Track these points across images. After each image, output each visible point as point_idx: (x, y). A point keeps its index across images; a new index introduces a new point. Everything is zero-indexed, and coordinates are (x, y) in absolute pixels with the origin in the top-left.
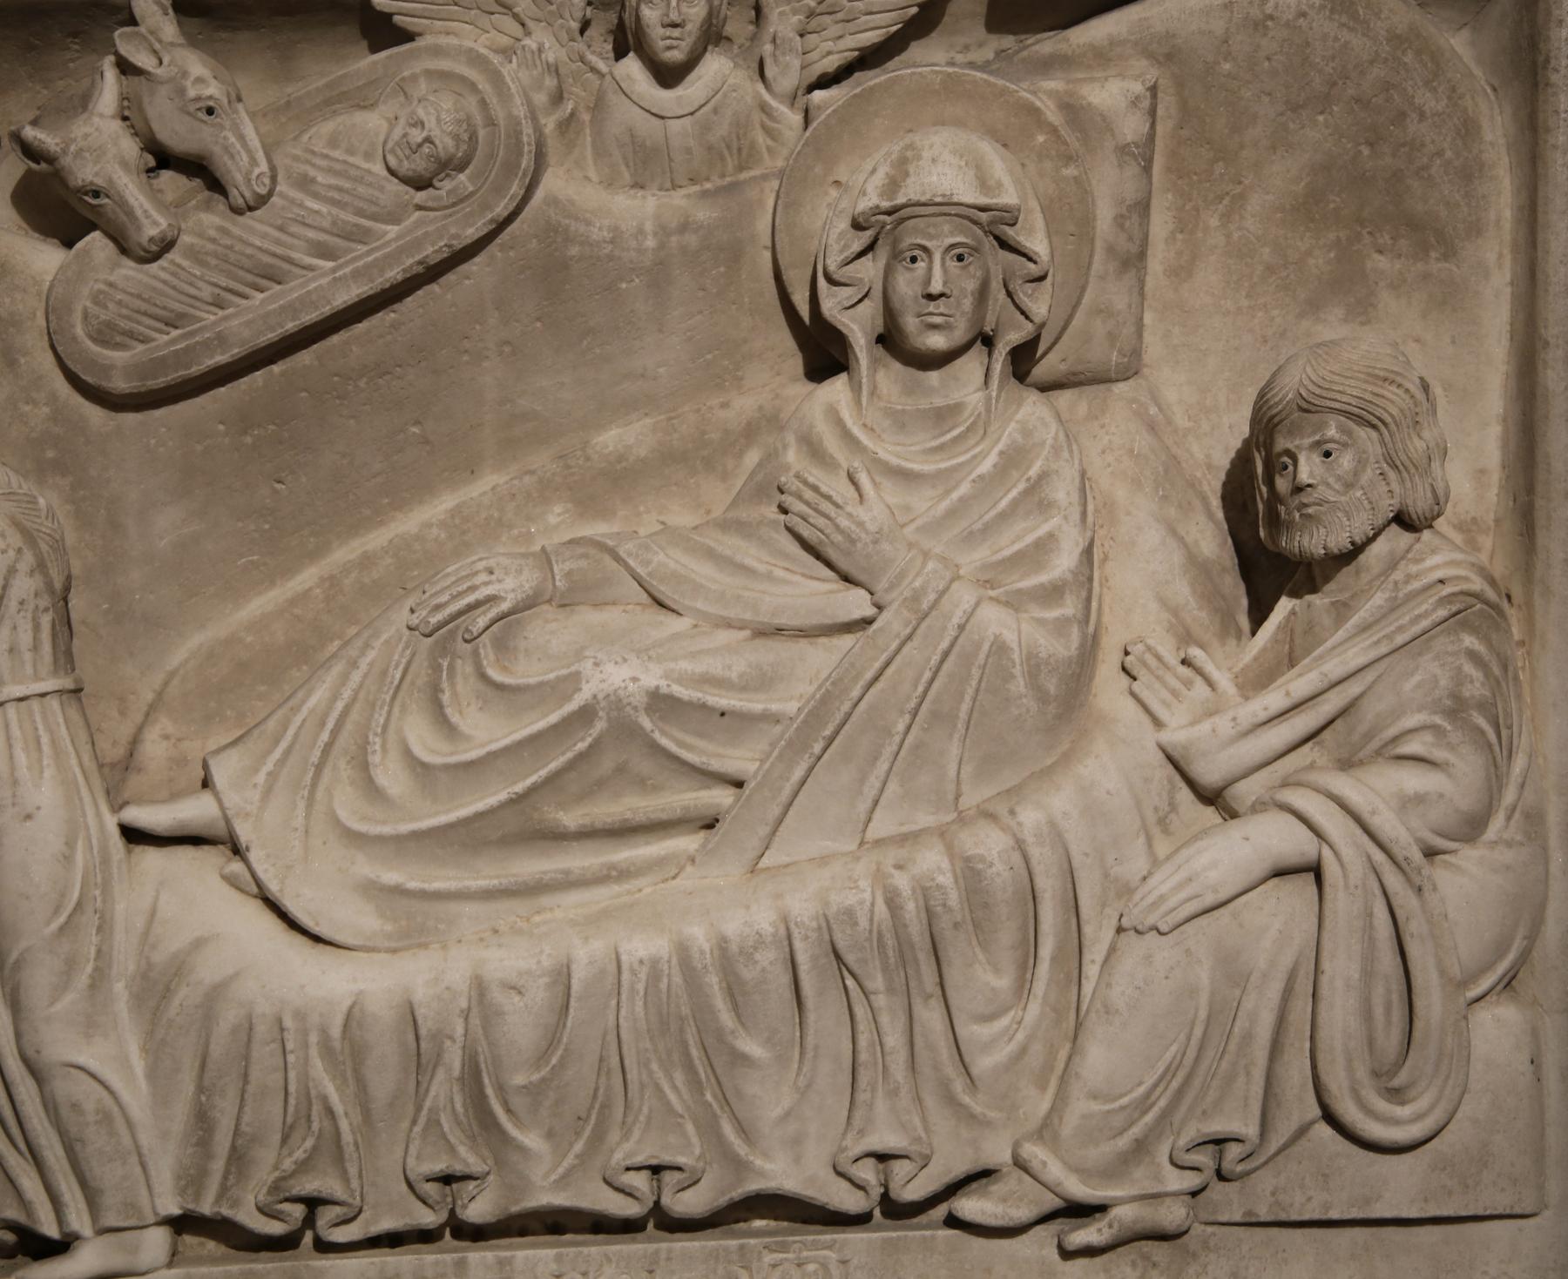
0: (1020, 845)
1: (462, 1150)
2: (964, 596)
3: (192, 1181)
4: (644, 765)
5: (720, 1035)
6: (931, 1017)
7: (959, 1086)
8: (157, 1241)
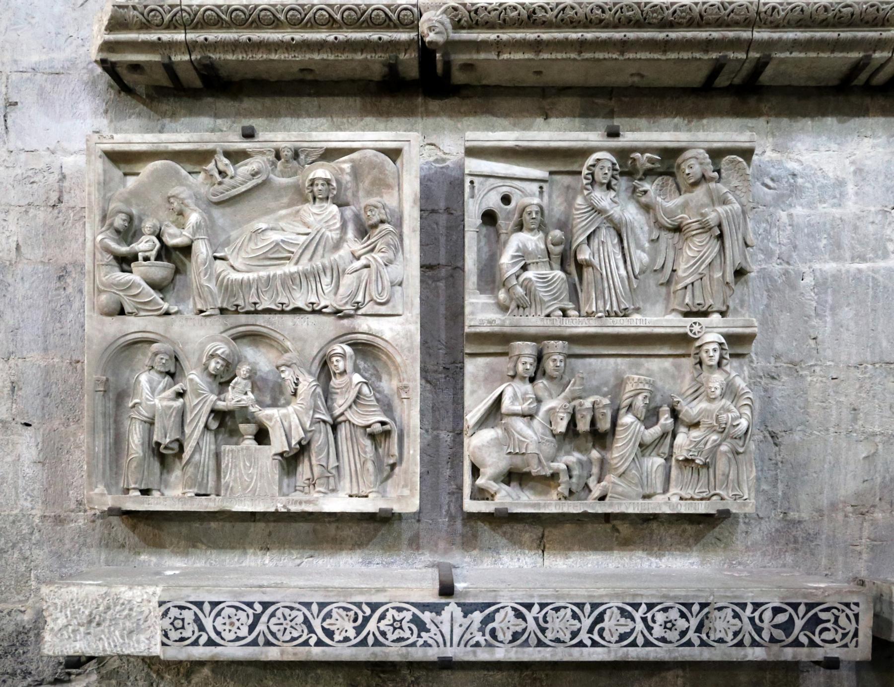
2: (324, 230)
3: (222, 302)
6: (319, 285)
8: (218, 311)
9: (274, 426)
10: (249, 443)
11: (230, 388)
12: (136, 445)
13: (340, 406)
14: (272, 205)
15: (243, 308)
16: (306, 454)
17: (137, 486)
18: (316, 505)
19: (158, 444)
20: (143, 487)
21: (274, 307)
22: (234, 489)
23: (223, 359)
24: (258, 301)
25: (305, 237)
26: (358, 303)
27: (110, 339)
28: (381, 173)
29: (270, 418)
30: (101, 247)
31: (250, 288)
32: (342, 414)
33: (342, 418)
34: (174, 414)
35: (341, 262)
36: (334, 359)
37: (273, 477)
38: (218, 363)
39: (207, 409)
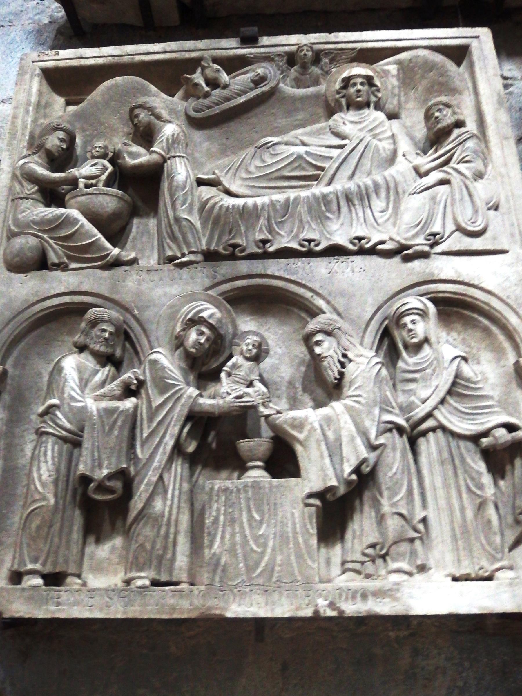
0: (385, 178)
1: (267, 234)
4: (304, 165)
5: (323, 212)
7: (375, 224)
9: (307, 438)
10: (257, 474)
11: (223, 375)
12: (43, 484)
13: (424, 402)
14: (282, 122)
15: (243, 251)
16: (367, 495)
17: (38, 566)
18: (396, 599)
19: (85, 480)
20: (48, 569)
21: (295, 245)
22: (230, 570)
23: (211, 327)
24: (270, 237)
25: (339, 151)
26: (435, 235)
27: (18, 305)
28: (442, 75)
29: (300, 425)
30: (22, 175)
31: (258, 217)
32: (429, 415)
33: (430, 423)
34: (119, 423)
35: (399, 178)
36: (407, 320)
37: (306, 542)
38: (202, 333)
39: (180, 411)
